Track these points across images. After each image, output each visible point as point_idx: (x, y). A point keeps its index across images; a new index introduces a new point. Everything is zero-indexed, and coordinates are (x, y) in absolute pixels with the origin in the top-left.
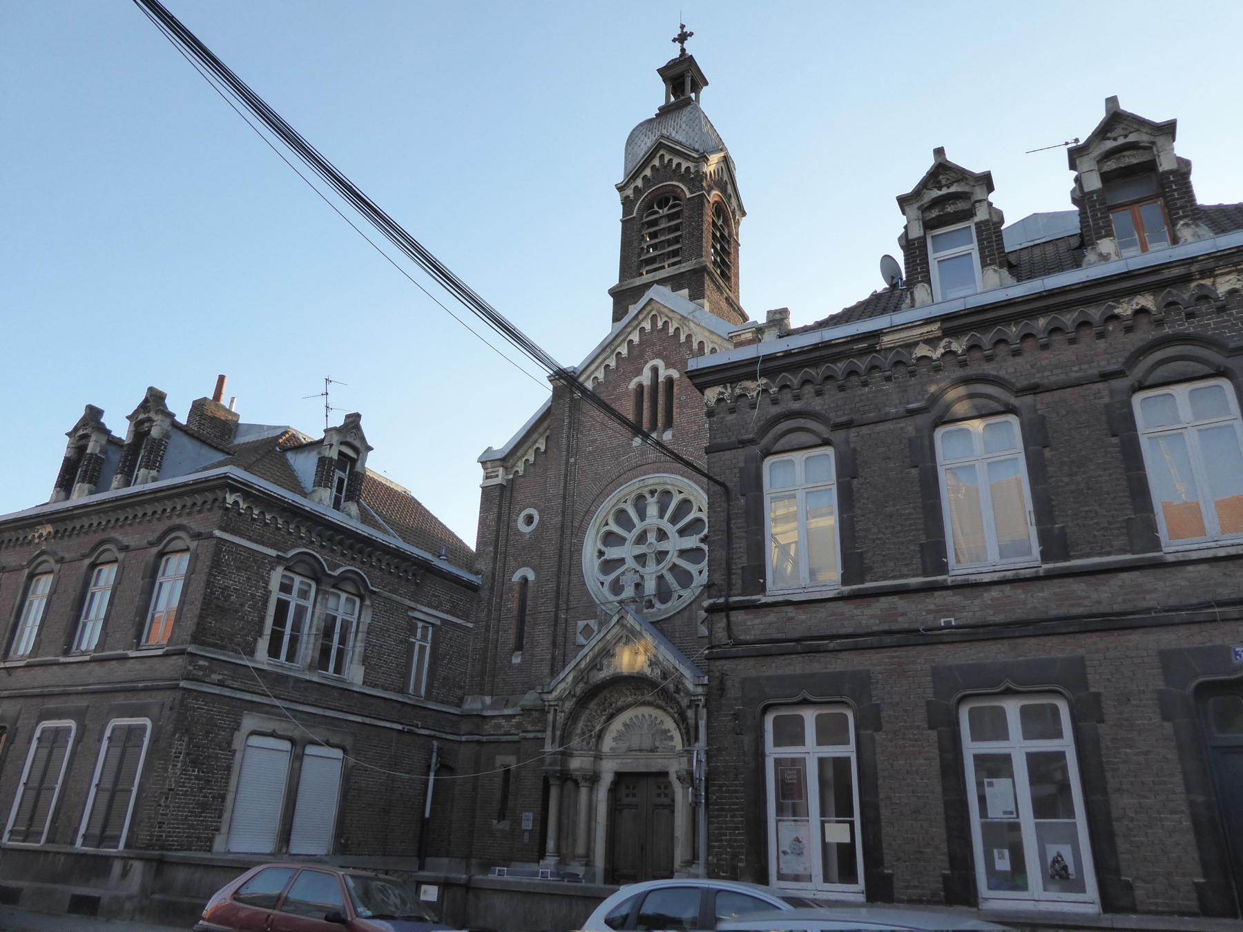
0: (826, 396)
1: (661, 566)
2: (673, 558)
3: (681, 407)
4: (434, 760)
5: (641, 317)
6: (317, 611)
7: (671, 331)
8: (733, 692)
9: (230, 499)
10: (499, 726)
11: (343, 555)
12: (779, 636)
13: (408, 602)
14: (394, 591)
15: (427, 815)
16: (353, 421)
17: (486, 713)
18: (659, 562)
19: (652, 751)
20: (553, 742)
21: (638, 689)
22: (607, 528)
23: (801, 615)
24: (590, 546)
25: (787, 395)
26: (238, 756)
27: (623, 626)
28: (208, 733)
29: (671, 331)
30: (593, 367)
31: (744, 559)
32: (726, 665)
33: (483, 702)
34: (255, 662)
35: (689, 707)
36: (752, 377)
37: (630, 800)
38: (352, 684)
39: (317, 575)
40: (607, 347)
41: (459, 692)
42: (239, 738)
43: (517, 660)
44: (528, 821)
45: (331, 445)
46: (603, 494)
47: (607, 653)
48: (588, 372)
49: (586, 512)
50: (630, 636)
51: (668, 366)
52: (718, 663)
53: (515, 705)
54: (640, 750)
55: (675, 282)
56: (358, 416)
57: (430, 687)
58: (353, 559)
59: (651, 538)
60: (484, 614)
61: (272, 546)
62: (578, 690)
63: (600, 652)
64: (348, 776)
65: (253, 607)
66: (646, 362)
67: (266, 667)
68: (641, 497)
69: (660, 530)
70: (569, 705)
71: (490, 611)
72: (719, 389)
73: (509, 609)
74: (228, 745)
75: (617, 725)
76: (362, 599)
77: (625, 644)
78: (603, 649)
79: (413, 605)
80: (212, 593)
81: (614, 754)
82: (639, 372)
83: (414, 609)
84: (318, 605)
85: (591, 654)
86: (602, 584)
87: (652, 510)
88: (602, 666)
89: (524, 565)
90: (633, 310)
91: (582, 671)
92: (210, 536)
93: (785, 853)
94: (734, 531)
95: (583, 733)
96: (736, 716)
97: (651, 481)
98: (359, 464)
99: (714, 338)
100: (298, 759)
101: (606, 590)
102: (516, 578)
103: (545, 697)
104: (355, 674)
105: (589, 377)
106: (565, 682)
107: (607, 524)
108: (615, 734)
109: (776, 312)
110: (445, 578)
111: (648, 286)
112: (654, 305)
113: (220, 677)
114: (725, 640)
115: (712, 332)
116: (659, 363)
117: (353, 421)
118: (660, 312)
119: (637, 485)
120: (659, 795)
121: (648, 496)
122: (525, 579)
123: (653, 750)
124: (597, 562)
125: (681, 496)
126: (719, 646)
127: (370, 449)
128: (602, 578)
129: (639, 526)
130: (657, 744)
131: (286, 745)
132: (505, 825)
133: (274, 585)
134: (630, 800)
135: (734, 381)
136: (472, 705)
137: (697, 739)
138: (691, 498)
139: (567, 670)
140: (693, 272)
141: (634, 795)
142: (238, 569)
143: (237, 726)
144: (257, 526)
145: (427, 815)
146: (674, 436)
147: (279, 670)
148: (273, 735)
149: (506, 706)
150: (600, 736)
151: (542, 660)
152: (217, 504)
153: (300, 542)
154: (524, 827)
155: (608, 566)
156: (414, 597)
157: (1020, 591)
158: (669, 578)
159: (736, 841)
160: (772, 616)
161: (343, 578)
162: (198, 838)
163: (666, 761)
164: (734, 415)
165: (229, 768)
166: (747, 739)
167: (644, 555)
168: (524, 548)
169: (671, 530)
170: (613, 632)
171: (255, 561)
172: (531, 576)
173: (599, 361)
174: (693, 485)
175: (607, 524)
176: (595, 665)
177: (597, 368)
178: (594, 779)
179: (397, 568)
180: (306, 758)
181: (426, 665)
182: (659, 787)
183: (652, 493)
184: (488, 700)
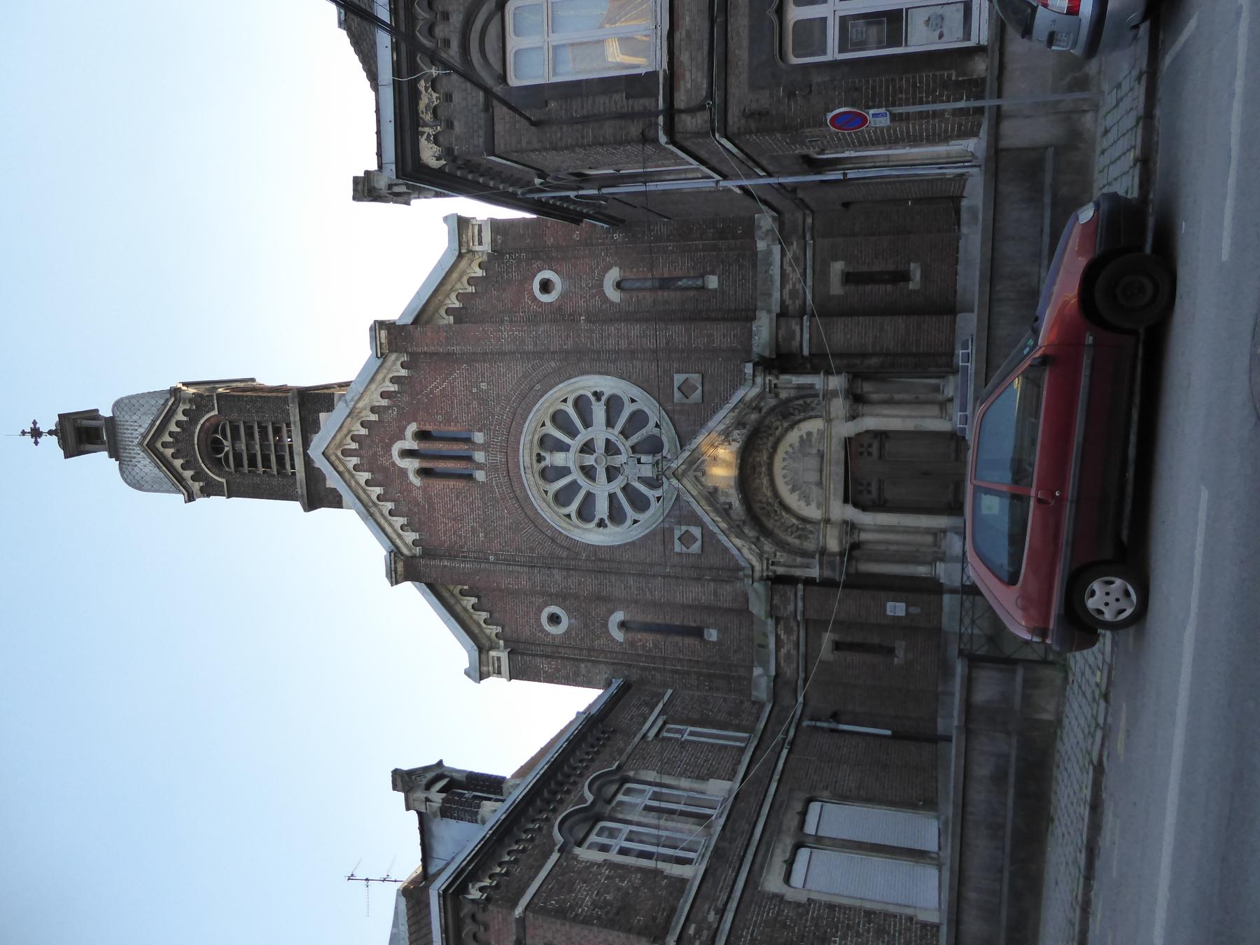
0: (450, 9)
1: (622, 448)
2: (614, 434)
3: (448, 421)
4: (825, 725)
5: (341, 468)
6: (636, 819)
7: (364, 431)
8: (763, 100)
9: (474, 893)
10: (788, 655)
11: (568, 792)
12: (706, 48)
13: (637, 740)
14: (621, 752)
15: (889, 732)
16: (404, 780)
17: (773, 673)
18: (618, 452)
19: (822, 457)
20: (808, 566)
21: (754, 467)
22: (573, 515)
23: (686, 22)
24: (592, 536)
25: (440, 31)
26: (814, 896)
27: (684, 473)
28: (785, 926)
29: (364, 431)
30: (389, 530)
31: (617, 97)
32: (734, 111)
33: (761, 676)
34: (695, 877)
35: (777, 395)
36: (415, 95)
37: (874, 488)
38: (730, 791)
39: (591, 817)
40: (369, 512)
41: (747, 704)
42: (790, 895)
43: (712, 635)
44: (896, 609)
45: (427, 800)
46: (535, 520)
47: (712, 495)
48: (394, 536)
49: (553, 540)
50: (696, 465)
51: (401, 437)
52: (730, 122)
53: (765, 623)
54: (821, 471)
55: (309, 427)
56: (397, 774)
57: (738, 728)
58: (575, 783)
59: (589, 460)
60: (658, 676)
61: (546, 856)
62: (750, 533)
63: (711, 504)
64: (843, 798)
65: (622, 879)
66: (394, 464)
67: (703, 867)
68: (544, 474)
69: (582, 451)
70: (768, 547)
71: (654, 669)
72: (423, 141)
73: (655, 646)
74: (803, 908)
75: (792, 500)
76: (626, 780)
77: (704, 474)
78: (707, 499)
79: (639, 736)
80: (599, 918)
81: (824, 504)
82: (403, 472)
83: (645, 736)
84: (629, 817)
85: (712, 514)
86: (635, 522)
87: (559, 459)
88: (725, 503)
89: (605, 625)
90: (333, 481)
91: (731, 527)
92: (521, 922)
93: (941, 36)
94: (585, 112)
95: (799, 537)
96: (791, 95)
97: (527, 459)
98: (456, 776)
99: (380, 377)
100: (819, 841)
101: (642, 517)
102: (619, 635)
103: (757, 575)
104: (719, 789)
105: (400, 536)
106: (742, 550)
107: (569, 516)
108: (802, 503)
109: (355, 190)
110: (612, 709)
111: (308, 461)
112: (330, 452)
113: (712, 913)
114: (706, 115)
115: (373, 379)
116: (397, 447)
117: (404, 780)
118: (341, 444)
119: (530, 476)
120: (870, 454)
121: (543, 464)
122: (622, 625)
123: (821, 455)
124: (611, 528)
125: (548, 423)
126: (712, 122)
127: (440, 762)
128: (629, 522)
129: (576, 475)
130: (814, 451)
131: (803, 854)
132: (900, 647)
133: (599, 857)
134: (874, 488)
135: (416, 122)
136: (762, 691)
137: (812, 386)
138: (551, 411)
139: (729, 545)
140: (301, 406)
141: (869, 484)
142: (570, 891)
143: (780, 898)
144: (517, 871)
145: (889, 732)
146: (480, 430)
147: (708, 854)
148: (790, 863)
149: (763, 646)
150: (804, 520)
151: (715, 594)
152: (480, 916)
153: (544, 832)
154: (903, 614)
155: (616, 515)
156: (630, 735)
157: (682, 83)
158: (635, 439)
159: (928, 84)
160: (684, 57)
161: (598, 794)
162: (922, 938)
163: (834, 440)
164: (456, 124)
165: (832, 907)
166: (817, 79)
167: (608, 469)
168: (586, 626)
169: (584, 436)
170: (689, 487)
171: (563, 874)
172: (619, 616)
173: (383, 522)
174: (538, 405)
175: (569, 516)
176: (725, 511)
177: (390, 525)
178: (850, 527)
179: (593, 746)
180: (821, 833)
181: (714, 731)
182: (862, 454)
183: (540, 458)
184: (757, 671)
